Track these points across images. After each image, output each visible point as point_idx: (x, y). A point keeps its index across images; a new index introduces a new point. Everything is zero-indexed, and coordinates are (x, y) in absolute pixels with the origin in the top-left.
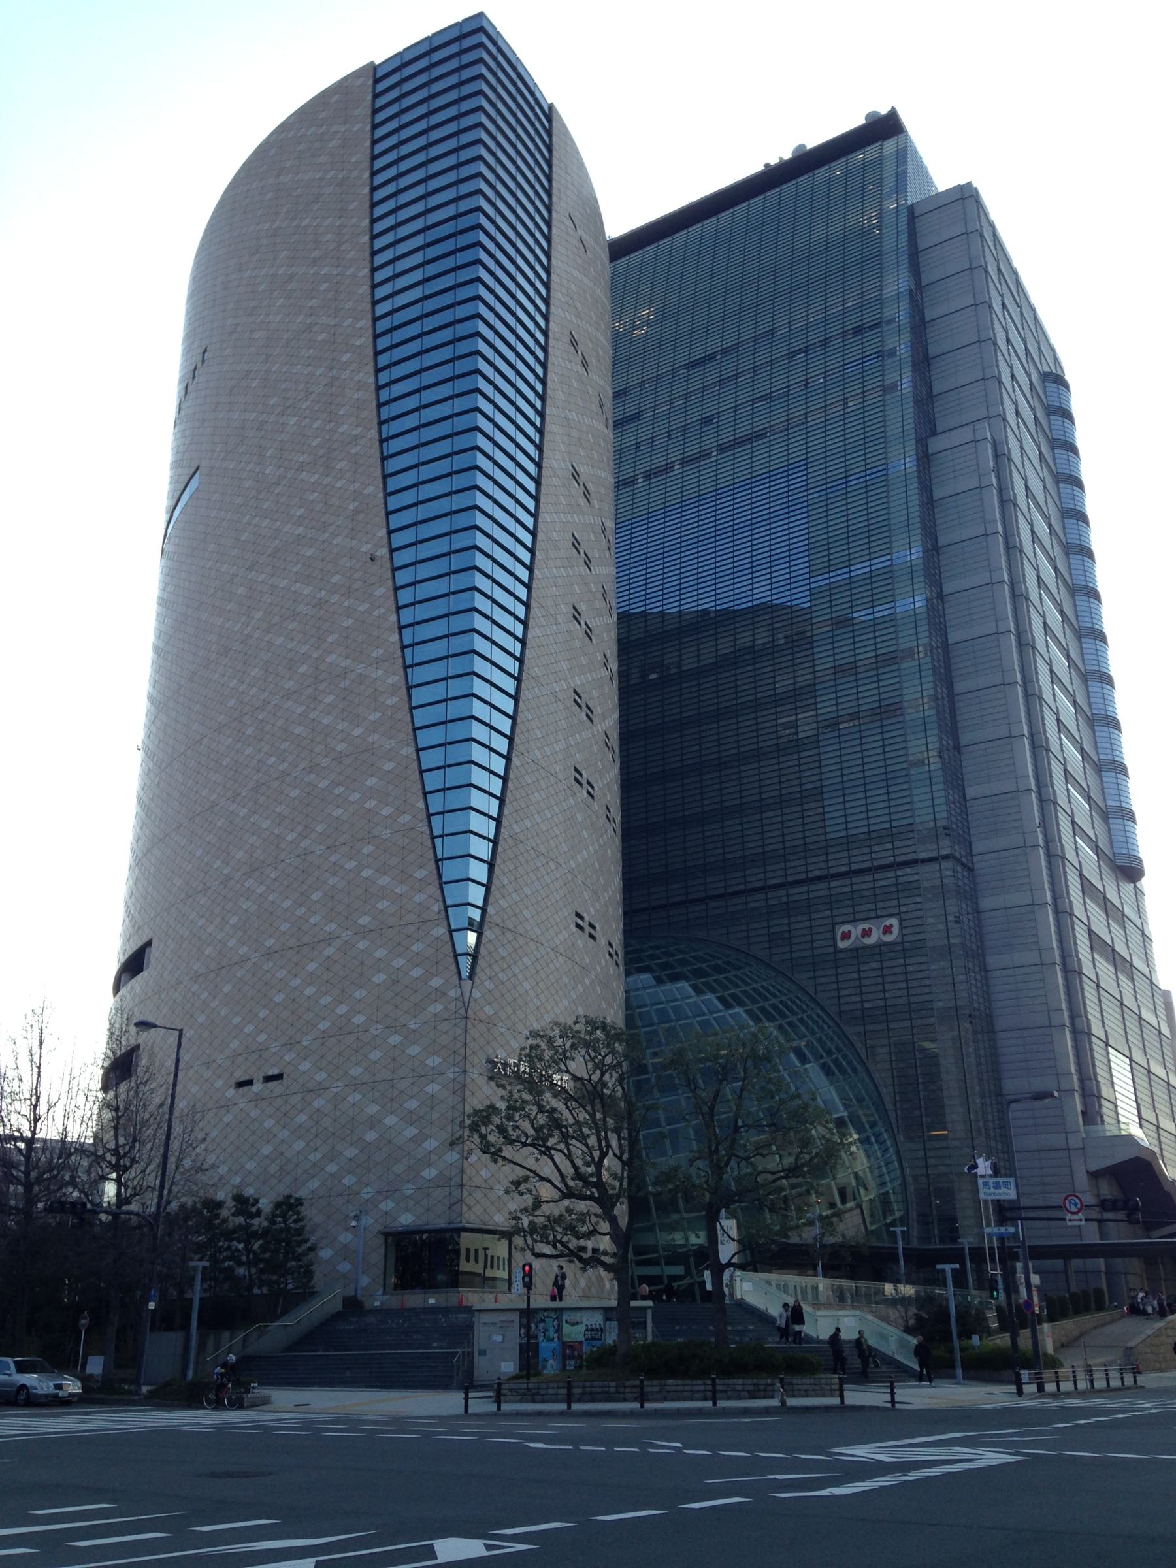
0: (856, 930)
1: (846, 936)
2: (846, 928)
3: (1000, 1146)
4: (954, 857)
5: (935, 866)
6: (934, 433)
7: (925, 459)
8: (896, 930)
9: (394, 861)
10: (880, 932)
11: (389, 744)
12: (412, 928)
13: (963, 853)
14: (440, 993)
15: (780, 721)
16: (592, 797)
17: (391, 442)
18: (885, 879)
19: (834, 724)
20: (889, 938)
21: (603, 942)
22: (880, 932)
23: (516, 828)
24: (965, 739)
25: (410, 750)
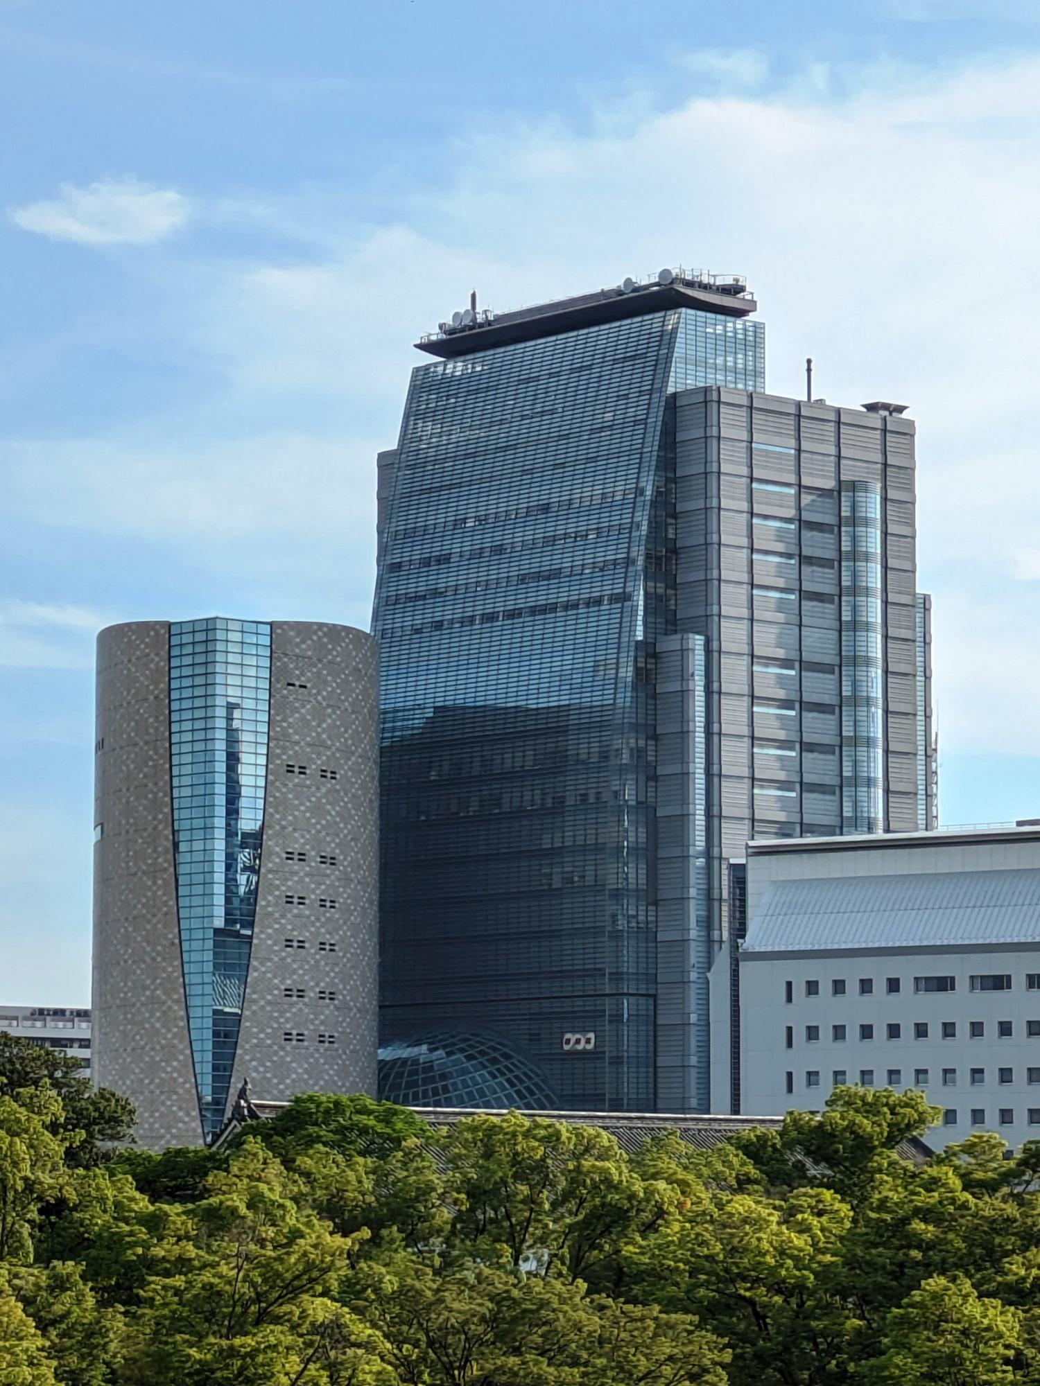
0: (573, 1037)
2: (568, 1036)
8: (593, 1041)
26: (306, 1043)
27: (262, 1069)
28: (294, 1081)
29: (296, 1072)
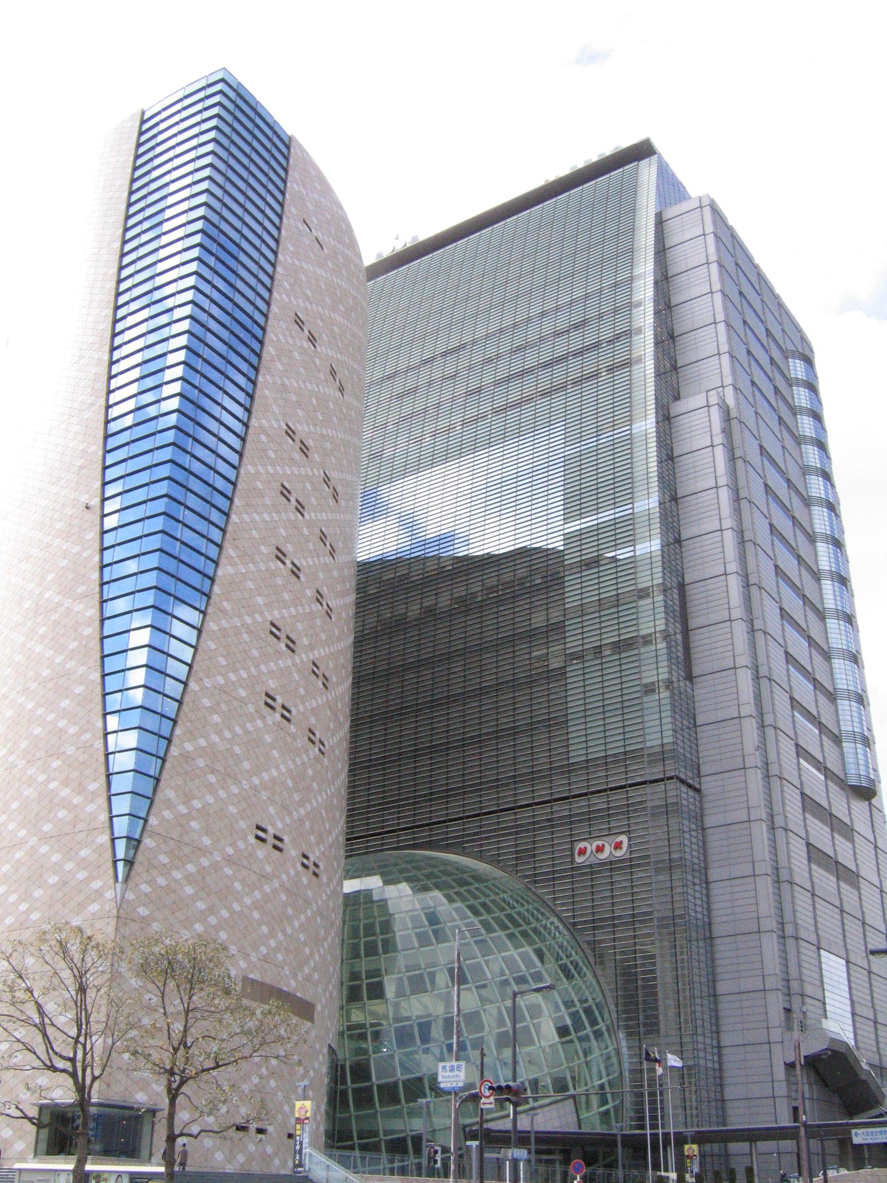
0: (591, 847)
1: (582, 852)
2: (582, 845)
3: (708, 1041)
4: (678, 778)
5: (660, 787)
6: (677, 398)
7: (666, 419)
9: (75, 774)
10: (610, 848)
11: (81, 670)
12: (83, 835)
13: (690, 775)
14: (99, 893)
15: (534, 654)
16: (288, 720)
17: (115, 408)
18: (618, 798)
19: (579, 656)
20: (618, 854)
21: (292, 852)
22: (610, 848)
23: (189, 747)
24: (696, 671)
25: (96, 676)
26: (293, 728)
27: (227, 734)
28: (272, 779)
29: (277, 767)
